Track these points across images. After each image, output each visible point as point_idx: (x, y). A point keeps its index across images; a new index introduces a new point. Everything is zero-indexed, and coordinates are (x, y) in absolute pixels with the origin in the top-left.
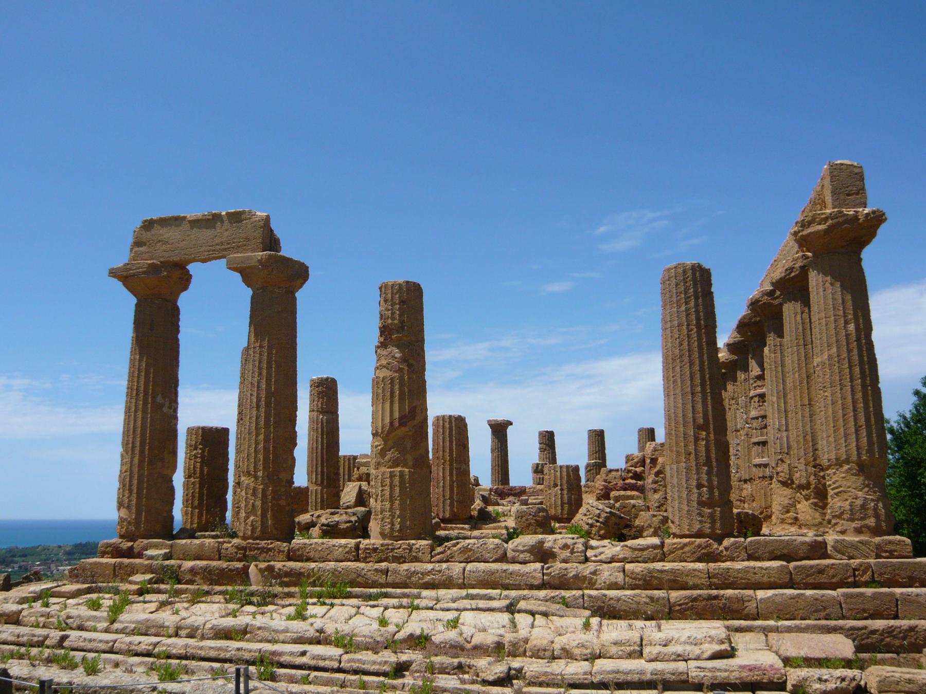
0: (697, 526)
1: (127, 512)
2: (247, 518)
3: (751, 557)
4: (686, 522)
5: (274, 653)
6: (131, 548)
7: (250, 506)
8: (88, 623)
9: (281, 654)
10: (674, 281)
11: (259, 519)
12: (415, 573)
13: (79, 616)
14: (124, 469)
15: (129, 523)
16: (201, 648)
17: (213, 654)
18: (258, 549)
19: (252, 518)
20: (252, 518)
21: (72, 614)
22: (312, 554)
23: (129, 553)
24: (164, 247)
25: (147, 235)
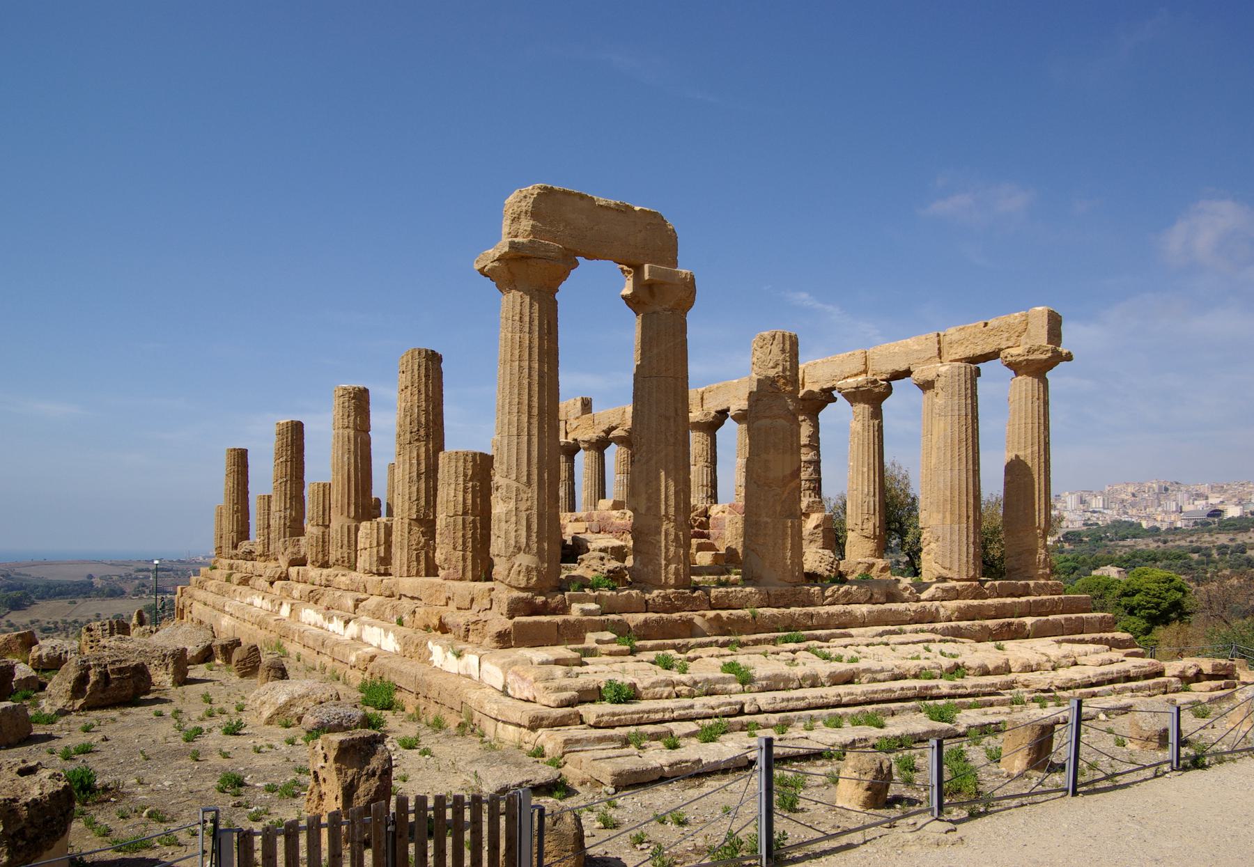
0: (972, 573)
1: (536, 559)
2: (667, 566)
3: (999, 596)
4: (964, 569)
5: (926, 688)
6: (545, 603)
7: (671, 554)
8: (718, 686)
9: (932, 688)
10: (962, 377)
11: (681, 566)
12: (833, 615)
13: (707, 680)
14: (523, 506)
15: (539, 572)
16: (876, 692)
17: (886, 696)
18: (684, 598)
19: (673, 566)
20: (673, 566)
21: (698, 679)
22: (734, 602)
23: (543, 610)
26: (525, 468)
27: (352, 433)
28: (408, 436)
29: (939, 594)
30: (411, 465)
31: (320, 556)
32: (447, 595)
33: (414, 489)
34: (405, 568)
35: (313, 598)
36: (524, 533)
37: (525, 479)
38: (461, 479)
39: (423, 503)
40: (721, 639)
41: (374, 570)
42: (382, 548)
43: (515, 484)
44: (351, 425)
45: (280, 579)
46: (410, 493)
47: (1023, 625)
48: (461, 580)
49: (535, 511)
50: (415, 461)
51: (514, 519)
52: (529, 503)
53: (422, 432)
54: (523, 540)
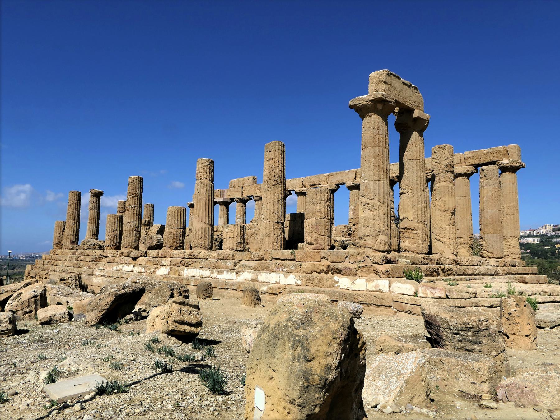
22: (443, 262)
24: (395, 91)
25: (389, 80)
26: (382, 196)
27: (208, 181)
28: (273, 182)
29: (495, 264)
30: (274, 196)
31: (175, 244)
32: (322, 256)
33: (276, 207)
34: (271, 246)
35: (186, 263)
36: (382, 226)
37: (382, 200)
38: (323, 202)
39: (280, 215)
40: (445, 278)
41: (235, 248)
42: (239, 238)
43: (378, 203)
44: (208, 178)
45: (141, 256)
46: (274, 209)
47: (525, 278)
48: (323, 249)
49: (386, 215)
50: (276, 194)
51: (377, 219)
52: (384, 211)
53: (280, 181)
54: (382, 228)
